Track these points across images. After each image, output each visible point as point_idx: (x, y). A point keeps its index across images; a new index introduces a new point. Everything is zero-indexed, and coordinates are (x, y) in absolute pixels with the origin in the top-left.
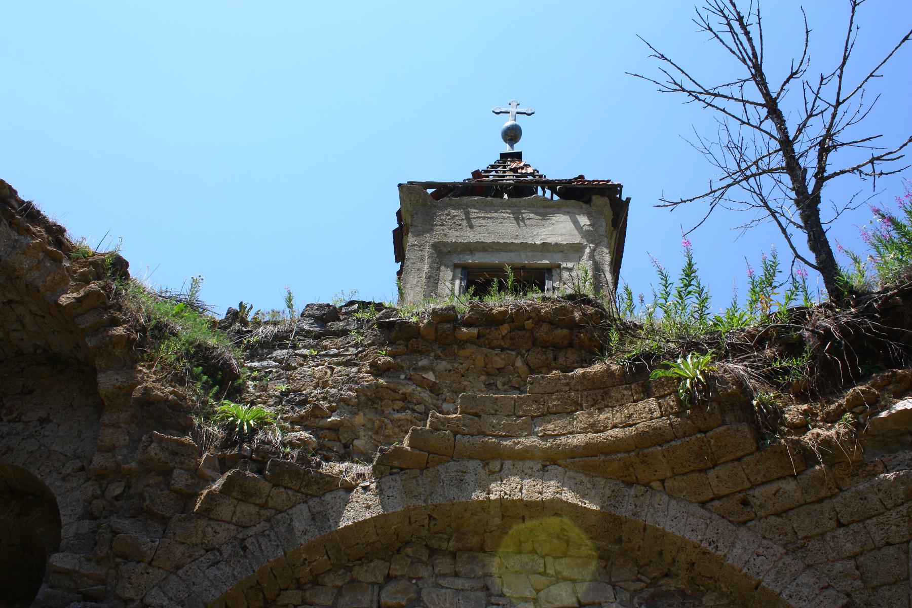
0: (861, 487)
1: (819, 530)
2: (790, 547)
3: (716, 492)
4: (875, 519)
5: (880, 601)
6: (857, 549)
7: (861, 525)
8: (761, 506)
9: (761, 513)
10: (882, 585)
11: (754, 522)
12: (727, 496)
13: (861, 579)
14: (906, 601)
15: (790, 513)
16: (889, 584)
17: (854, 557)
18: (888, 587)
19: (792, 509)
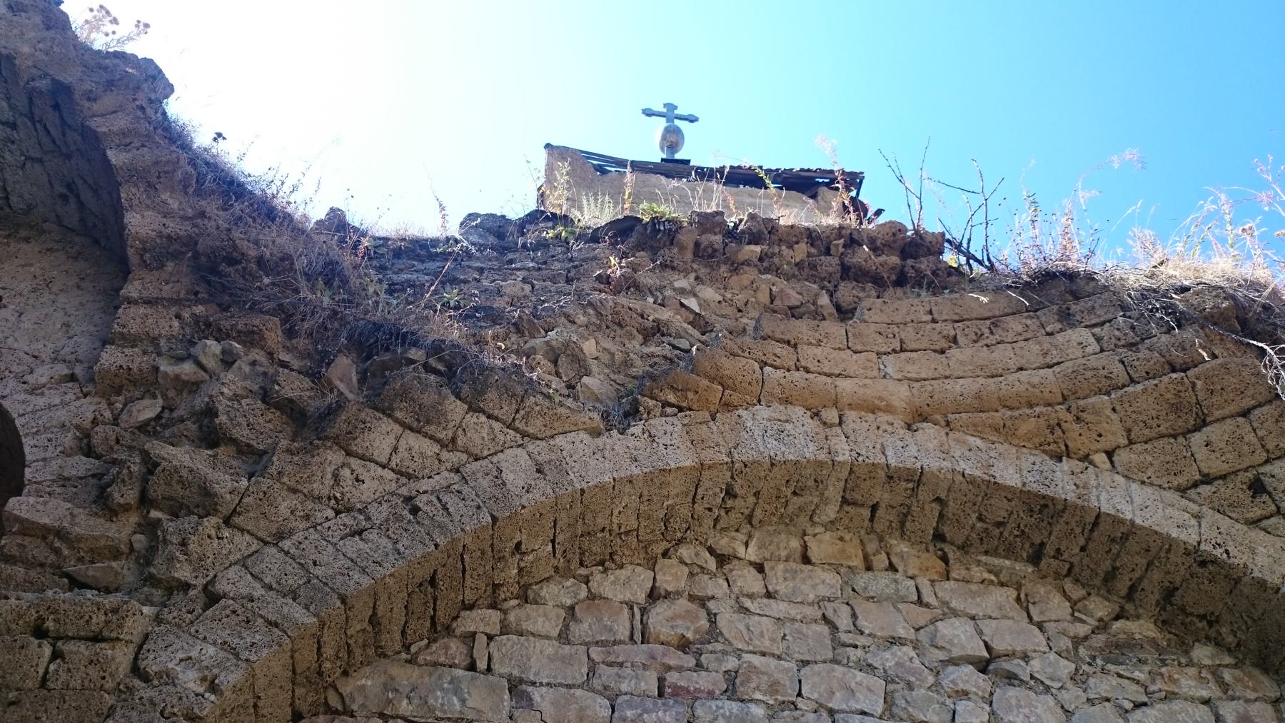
3: (1206, 471)
11: (1273, 520)
12: (1224, 477)
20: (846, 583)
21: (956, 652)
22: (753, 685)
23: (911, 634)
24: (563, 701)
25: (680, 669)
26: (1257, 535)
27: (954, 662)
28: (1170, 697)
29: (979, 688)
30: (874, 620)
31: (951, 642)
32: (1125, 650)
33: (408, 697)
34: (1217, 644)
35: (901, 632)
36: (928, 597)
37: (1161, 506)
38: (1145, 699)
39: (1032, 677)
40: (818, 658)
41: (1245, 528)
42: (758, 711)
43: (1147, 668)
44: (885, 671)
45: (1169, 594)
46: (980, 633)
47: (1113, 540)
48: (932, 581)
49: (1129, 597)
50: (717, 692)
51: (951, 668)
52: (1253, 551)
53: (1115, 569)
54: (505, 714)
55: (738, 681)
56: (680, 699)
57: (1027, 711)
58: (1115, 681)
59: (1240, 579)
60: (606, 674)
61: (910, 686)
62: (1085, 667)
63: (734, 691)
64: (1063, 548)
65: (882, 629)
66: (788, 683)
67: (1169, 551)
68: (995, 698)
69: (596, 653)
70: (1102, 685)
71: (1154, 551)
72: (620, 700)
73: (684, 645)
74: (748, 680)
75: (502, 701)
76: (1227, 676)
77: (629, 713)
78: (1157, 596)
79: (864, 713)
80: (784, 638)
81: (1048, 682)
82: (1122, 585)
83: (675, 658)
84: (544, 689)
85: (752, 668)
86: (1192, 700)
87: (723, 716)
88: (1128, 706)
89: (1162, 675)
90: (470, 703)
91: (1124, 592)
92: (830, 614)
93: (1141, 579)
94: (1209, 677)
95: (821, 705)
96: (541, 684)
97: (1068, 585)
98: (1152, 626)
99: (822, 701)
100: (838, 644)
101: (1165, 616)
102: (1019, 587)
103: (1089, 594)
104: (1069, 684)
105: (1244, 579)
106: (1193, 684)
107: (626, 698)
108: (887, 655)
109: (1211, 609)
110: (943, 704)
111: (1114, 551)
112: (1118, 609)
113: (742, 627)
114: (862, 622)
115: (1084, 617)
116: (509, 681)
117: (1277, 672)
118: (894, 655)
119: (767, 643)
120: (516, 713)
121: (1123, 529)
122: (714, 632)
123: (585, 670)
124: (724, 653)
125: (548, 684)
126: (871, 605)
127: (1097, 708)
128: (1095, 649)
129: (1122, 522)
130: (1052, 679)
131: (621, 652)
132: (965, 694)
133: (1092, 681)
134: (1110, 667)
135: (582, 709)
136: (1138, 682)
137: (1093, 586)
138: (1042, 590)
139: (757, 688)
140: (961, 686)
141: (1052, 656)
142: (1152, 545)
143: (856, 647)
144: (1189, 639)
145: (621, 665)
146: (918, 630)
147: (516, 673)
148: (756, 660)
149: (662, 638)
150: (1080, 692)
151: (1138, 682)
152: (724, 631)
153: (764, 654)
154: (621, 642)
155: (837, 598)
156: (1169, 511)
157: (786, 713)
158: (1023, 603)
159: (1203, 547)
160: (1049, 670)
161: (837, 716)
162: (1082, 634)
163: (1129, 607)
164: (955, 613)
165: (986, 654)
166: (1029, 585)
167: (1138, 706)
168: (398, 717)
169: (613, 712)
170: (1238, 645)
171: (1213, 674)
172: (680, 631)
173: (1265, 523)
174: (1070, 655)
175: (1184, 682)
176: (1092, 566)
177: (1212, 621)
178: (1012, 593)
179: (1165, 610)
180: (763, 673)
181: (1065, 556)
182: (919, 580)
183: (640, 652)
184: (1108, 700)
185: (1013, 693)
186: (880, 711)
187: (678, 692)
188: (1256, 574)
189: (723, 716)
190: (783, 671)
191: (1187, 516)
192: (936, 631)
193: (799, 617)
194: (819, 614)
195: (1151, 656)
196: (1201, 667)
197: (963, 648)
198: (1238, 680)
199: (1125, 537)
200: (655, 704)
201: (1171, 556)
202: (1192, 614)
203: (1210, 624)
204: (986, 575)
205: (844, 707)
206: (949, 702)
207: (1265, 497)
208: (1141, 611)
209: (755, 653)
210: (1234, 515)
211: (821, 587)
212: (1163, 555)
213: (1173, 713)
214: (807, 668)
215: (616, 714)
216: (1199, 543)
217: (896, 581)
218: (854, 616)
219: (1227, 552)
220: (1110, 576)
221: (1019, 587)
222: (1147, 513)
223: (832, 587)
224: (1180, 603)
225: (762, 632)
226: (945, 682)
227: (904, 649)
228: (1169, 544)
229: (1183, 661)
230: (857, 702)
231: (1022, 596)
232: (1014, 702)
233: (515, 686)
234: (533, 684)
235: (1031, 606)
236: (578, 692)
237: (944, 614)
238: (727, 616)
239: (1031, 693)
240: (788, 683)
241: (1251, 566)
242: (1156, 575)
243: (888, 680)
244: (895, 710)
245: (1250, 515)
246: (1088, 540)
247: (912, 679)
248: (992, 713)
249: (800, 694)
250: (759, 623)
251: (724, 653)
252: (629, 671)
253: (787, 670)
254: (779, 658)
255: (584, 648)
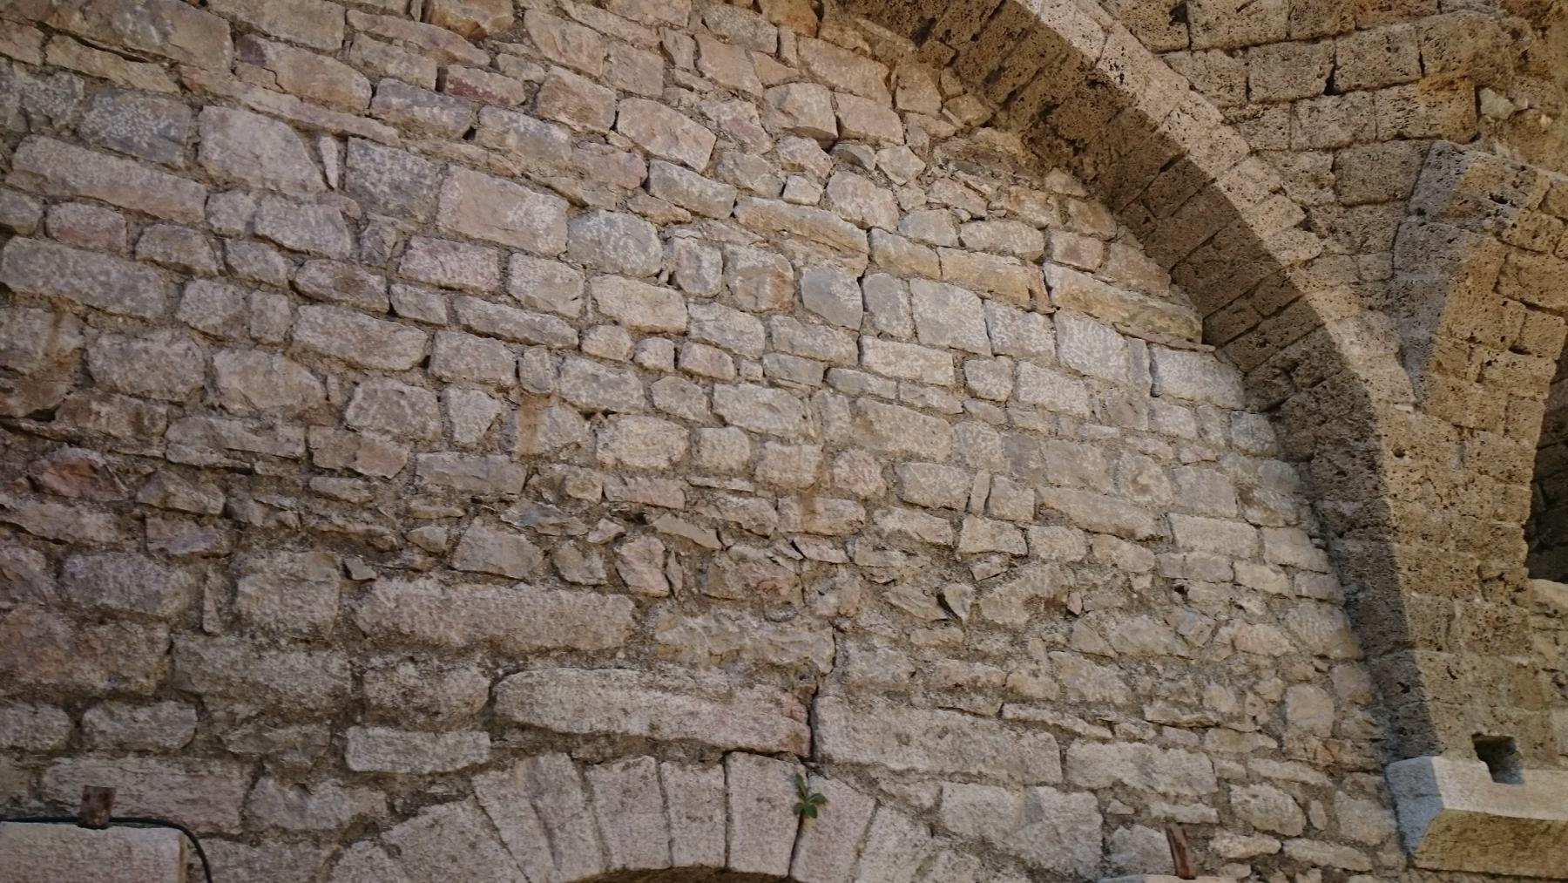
0: (1397, 28)
1: (1292, 93)
2: (1233, 112)
4: (1395, 90)
5: (1352, 228)
6: (1344, 137)
7: (1368, 95)
8: (1207, 28)
9: (1202, 40)
10: (1361, 204)
11: (1181, 54)
13: (1334, 187)
14: (1392, 234)
15: (1253, 51)
16: (1375, 202)
17: (1334, 150)
18: (1370, 208)
19: (1257, 45)
20: (697, 11)
21: (803, 122)
22: (559, 104)
23: (758, 90)
24: (306, 67)
25: (468, 64)
26: (1158, 66)
27: (799, 133)
28: (1009, 216)
29: (817, 166)
30: (720, 64)
31: (800, 109)
32: (981, 161)
33: (83, 12)
34: (1075, 174)
35: (747, 85)
36: (789, 53)
37: (1074, 7)
38: (984, 213)
39: (877, 167)
40: (644, 92)
41: (1150, 56)
42: (561, 135)
43: (997, 184)
44: (719, 125)
45: (1048, 109)
46: (835, 107)
47: (1010, 35)
48: (798, 35)
49: (1005, 105)
50: (513, 102)
51: (793, 139)
52: (1148, 83)
53: (1002, 69)
54: (225, 64)
55: (540, 95)
56: (463, 99)
57: (861, 201)
58: (960, 189)
59: (1123, 108)
60: (368, 48)
61: (743, 147)
62: (935, 170)
63: (534, 106)
64: (953, 32)
65: (727, 76)
66: (602, 112)
67: (1064, 61)
68: (832, 180)
69: (356, 18)
70: (945, 191)
71: (1048, 57)
72: (384, 82)
73: (477, 37)
74: (554, 97)
75: (222, 48)
76: (1072, 207)
77: (395, 101)
78: (1034, 110)
79: (685, 165)
80: (606, 59)
81: (892, 177)
82: (1002, 90)
83: (463, 49)
84: (281, 47)
85: (560, 83)
86: (1030, 223)
87: (517, 131)
88: (965, 216)
89: (1009, 193)
90: (175, 39)
91: (1002, 98)
92: (669, 44)
93: (1024, 87)
94: (1055, 204)
95: (637, 146)
96: (278, 39)
97: (946, 76)
98: (1018, 141)
99: (639, 140)
100: (671, 81)
101: (1035, 133)
102: (892, 65)
103: (965, 92)
104: (913, 183)
105: (1128, 110)
106: (1036, 207)
107: (393, 82)
108: (726, 107)
109: (1083, 135)
110: (775, 174)
111: (1007, 48)
112: (989, 116)
113: (556, 33)
114: (704, 63)
115: (951, 116)
116: (232, 24)
117: (1120, 213)
118: (733, 109)
119: (585, 60)
120: (241, 67)
121: (1025, 25)
122: (518, 30)
123: (340, 36)
124: (528, 58)
125: (288, 42)
126: (719, 45)
127: (933, 213)
128: (951, 153)
129: (1026, 15)
130: (897, 174)
131: (393, 26)
132: (801, 169)
133: (937, 184)
134: (961, 174)
135: (332, 82)
136: (983, 195)
137: (972, 84)
138: (916, 76)
139: (564, 109)
140: (799, 160)
141: (905, 150)
142: (1050, 50)
143: (691, 89)
144: (1049, 163)
145: (390, 41)
146: (767, 87)
147: (242, 16)
148: (568, 77)
149: (449, 21)
150: (922, 194)
151: (983, 195)
152: (533, 32)
153: (579, 72)
154: (392, 13)
155: (681, 27)
156: (1081, 16)
157: (594, 145)
158: (892, 85)
159: (1100, 65)
160: (897, 164)
161: (653, 162)
162: (943, 134)
163: (1002, 116)
164: (814, 78)
165: (835, 132)
166: (904, 67)
167: (974, 219)
168: (67, 33)
169: (374, 94)
170: (1095, 179)
171: (1060, 202)
172: (474, 18)
173: (1172, 55)
174: (925, 153)
175: (1028, 204)
176: (979, 61)
177: (1079, 148)
178: (883, 70)
179: (1036, 126)
180: (574, 94)
181: (953, 42)
182: (783, 29)
183: (418, 32)
184: (947, 207)
185: (851, 178)
186: (703, 166)
187: (461, 90)
188: (1141, 107)
189: (517, 131)
190: (600, 98)
191: (1097, 26)
192: (788, 93)
193: (630, 38)
194: (656, 41)
195: (1005, 172)
196: (1051, 193)
197: (812, 119)
198: (1081, 213)
199: (1025, 34)
200: (431, 98)
201: (1065, 67)
202: (1062, 137)
203: (1076, 151)
204: (860, 43)
205: (664, 153)
206: (781, 174)
207: (1182, 27)
208: (1012, 122)
209: (567, 68)
210: (1143, 39)
211: (665, 8)
212: (1056, 64)
213: (1007, 232)
214: (629, 101)
215: (377, 98)
216: (1098, 60)
217: (756, 24)
218: (697, 53)
219: (1122, 77)
220: (994, 77)
221: (892, 65)
222: (1057, 13)
223: (678, 12)
224: (1054, 121)
225: (580, 46)
226: (783, 152)
227: (747, 105)
228: (1067, 53)
229: (1036, 184)
230: (679, 151)
231: (893, 77)
232: (850, 189)
233: (241, 33)
234: (267, 36)
235: (899, 91)
236: (329, 61)
237: (802, 77)
238: (540, 15)
239: (871, 184)
240: (602, 112)
241: (1139, 97)
242: (1041, 86)
243: (720, 135)
244: (720, 170)
245: (1161, 43)
246: (984, 28)
247: (747, 140)
248: (825, 195)
249: (614, 128)
250: (579, 33)
251: (528, 58)
252: (400, 51)
253: (604, 97)
254: (597, 81)
255: (341, 8)
